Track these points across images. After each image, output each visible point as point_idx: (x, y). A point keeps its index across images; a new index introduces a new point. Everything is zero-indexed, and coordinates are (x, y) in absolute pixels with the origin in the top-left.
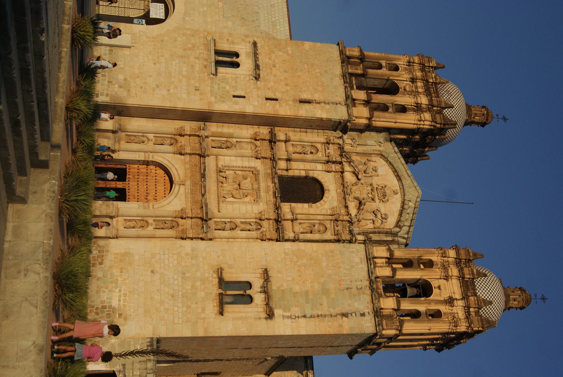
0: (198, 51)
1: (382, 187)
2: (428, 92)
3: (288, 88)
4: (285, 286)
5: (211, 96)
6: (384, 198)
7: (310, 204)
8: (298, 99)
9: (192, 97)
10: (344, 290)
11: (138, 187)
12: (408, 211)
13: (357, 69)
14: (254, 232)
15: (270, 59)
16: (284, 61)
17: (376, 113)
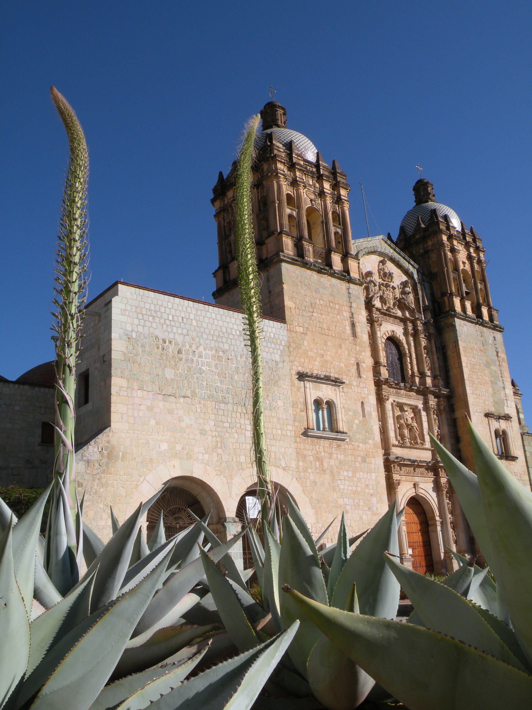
0: (323, 454)
3: (343, 345)
4: (491, 400)
9: (373, 466)
15: (315, 361)
16: (314, 340)
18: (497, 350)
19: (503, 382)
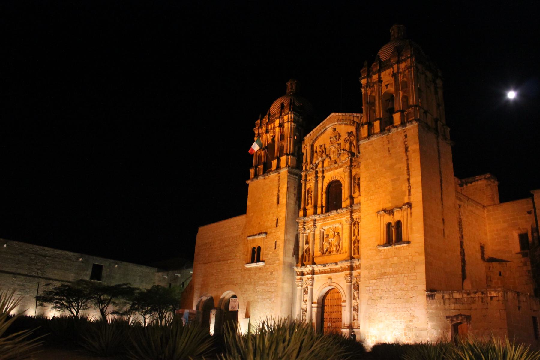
2: (273, 121)
3: (271, 212)
4: (389, 197)
5: (275, 263)
7: (342, 188)
8: (277, 205)
10: (390, 154)
11: (335, 312)
12: (344, 119)
13: (261, 169)
17: (285, 152)
18: (407, 146)
19: (409, 175)
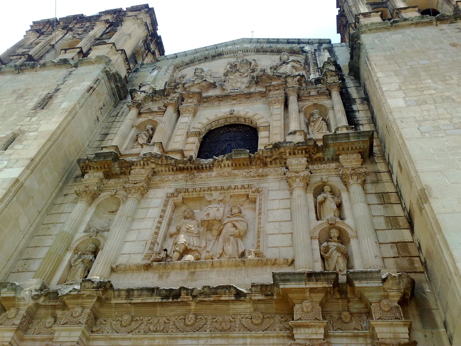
1: (230, 68)
6: (251, 64)
14: (344, 196)
